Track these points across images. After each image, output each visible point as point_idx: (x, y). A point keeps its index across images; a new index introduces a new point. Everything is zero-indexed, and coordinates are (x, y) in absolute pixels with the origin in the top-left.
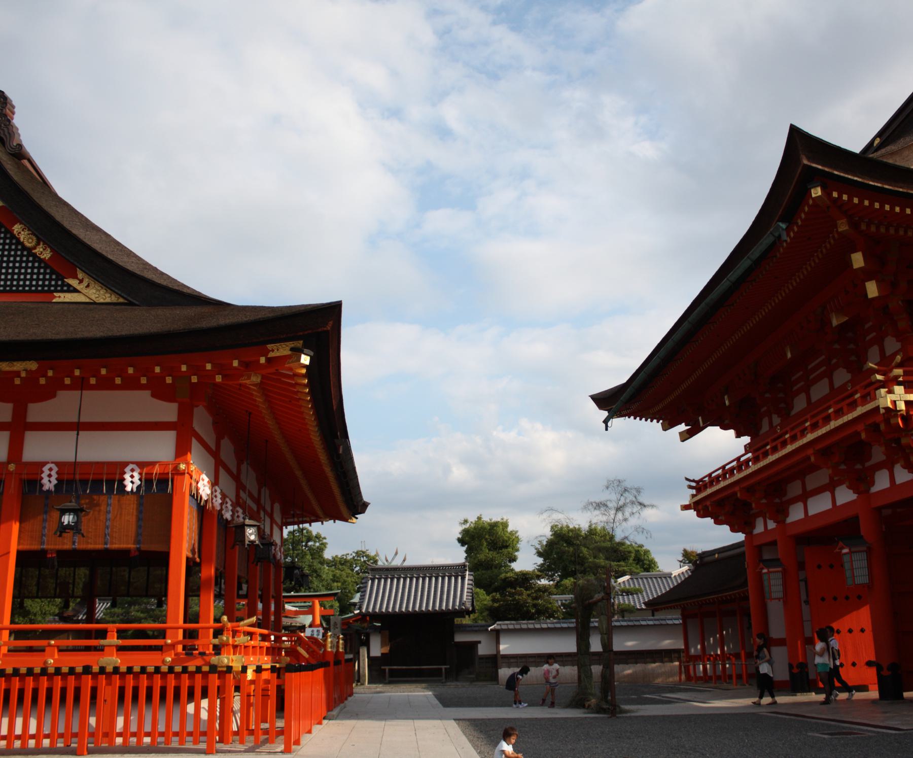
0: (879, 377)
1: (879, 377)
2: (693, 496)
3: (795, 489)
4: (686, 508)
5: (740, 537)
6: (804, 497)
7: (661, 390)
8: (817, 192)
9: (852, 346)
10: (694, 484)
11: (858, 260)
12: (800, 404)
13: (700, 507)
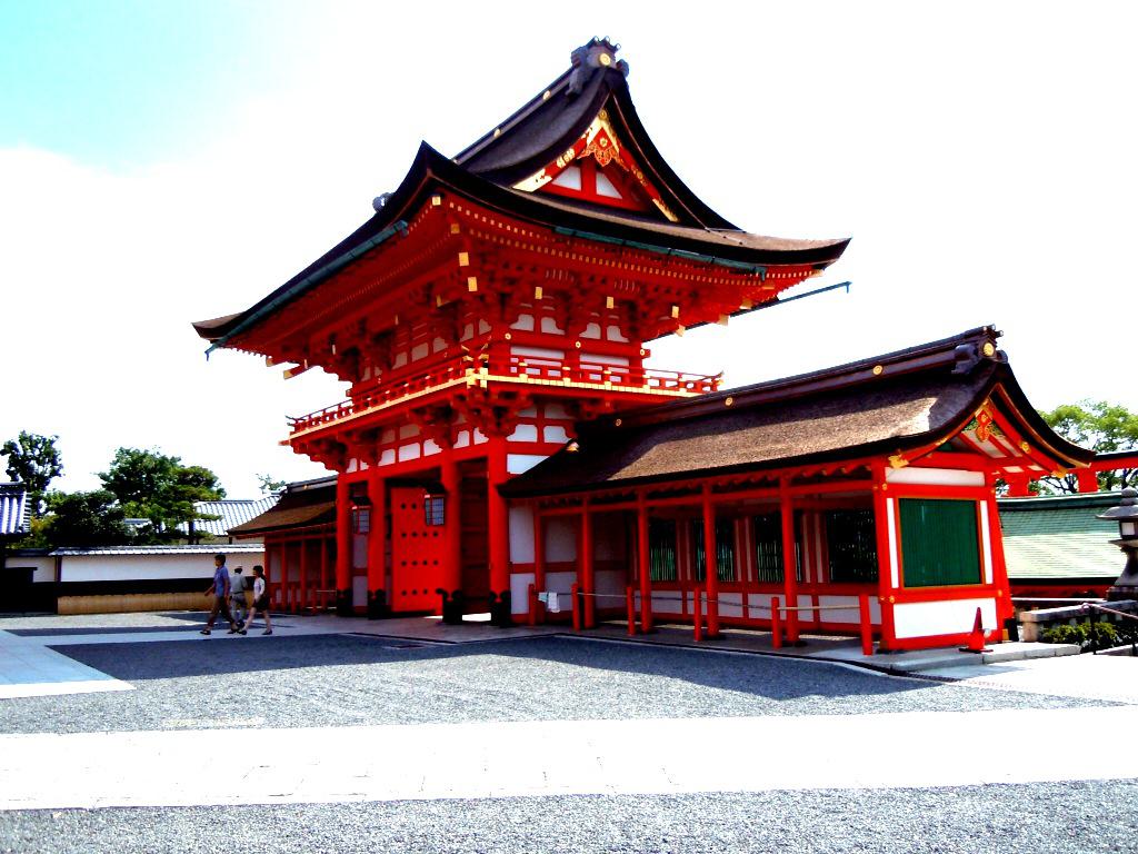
0: (469, 359)
1: (469, 359)
2: (292, 433)
3: (389, 437)
4: (284, 443)
6: (397, 445)
7: (273, 328)
8: (437, 201)
10: (294, 422)
11: (464, 259)
12: (401, 360)
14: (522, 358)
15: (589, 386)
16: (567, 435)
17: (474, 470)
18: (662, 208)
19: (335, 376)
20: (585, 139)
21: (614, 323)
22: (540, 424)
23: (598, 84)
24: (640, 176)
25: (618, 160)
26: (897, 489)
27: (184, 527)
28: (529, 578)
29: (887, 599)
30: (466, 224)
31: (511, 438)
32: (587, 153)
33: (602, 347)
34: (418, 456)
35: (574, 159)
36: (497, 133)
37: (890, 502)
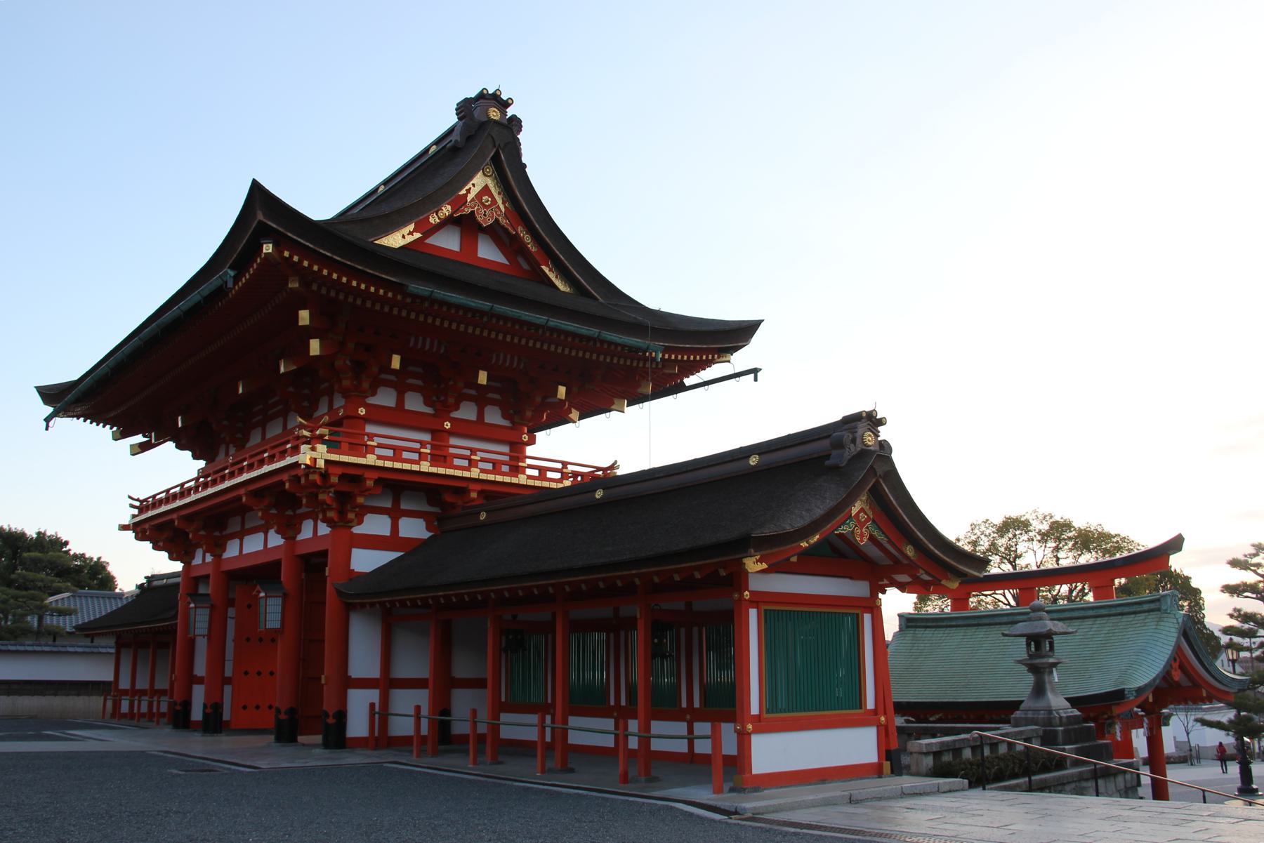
0: (306, 433)
1: (306, 433)
2: (134, 516)
3: (234, 526)
4: (124, 528)
5: (177, 566)
6: (241, 535)
7: (121, 393)
8: (268, 248)
9: (306, 391)
10: (137, 504)
11: (304, 317)
12: (256, 438)
13: (139, 529)
14: (371, 436)
15: (450, 472)
16: (428, 529)
17: (313, 564)
18: (552, 276)
19: (188, 454)
20: (466, 195)
21: (493, 402)
22: (395, 514)
23: (485, 133)
24: (527, 239)
25: (503, 222)
26: (760, 599)
27: (33, 621)
28: (373, 695)
29: (744, 727)
30: (306, 277)
31: (357, 530)
32: (467, 211)
33: (478, 430)
34: (261, 548)
35: (451, 216)
36: (382, 188)
37: (753, 613)
